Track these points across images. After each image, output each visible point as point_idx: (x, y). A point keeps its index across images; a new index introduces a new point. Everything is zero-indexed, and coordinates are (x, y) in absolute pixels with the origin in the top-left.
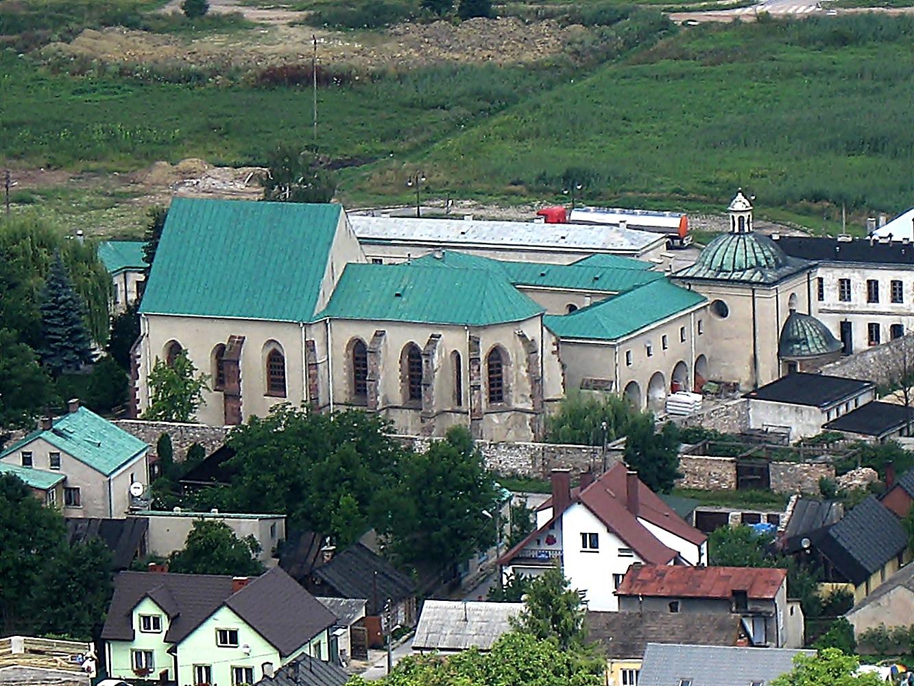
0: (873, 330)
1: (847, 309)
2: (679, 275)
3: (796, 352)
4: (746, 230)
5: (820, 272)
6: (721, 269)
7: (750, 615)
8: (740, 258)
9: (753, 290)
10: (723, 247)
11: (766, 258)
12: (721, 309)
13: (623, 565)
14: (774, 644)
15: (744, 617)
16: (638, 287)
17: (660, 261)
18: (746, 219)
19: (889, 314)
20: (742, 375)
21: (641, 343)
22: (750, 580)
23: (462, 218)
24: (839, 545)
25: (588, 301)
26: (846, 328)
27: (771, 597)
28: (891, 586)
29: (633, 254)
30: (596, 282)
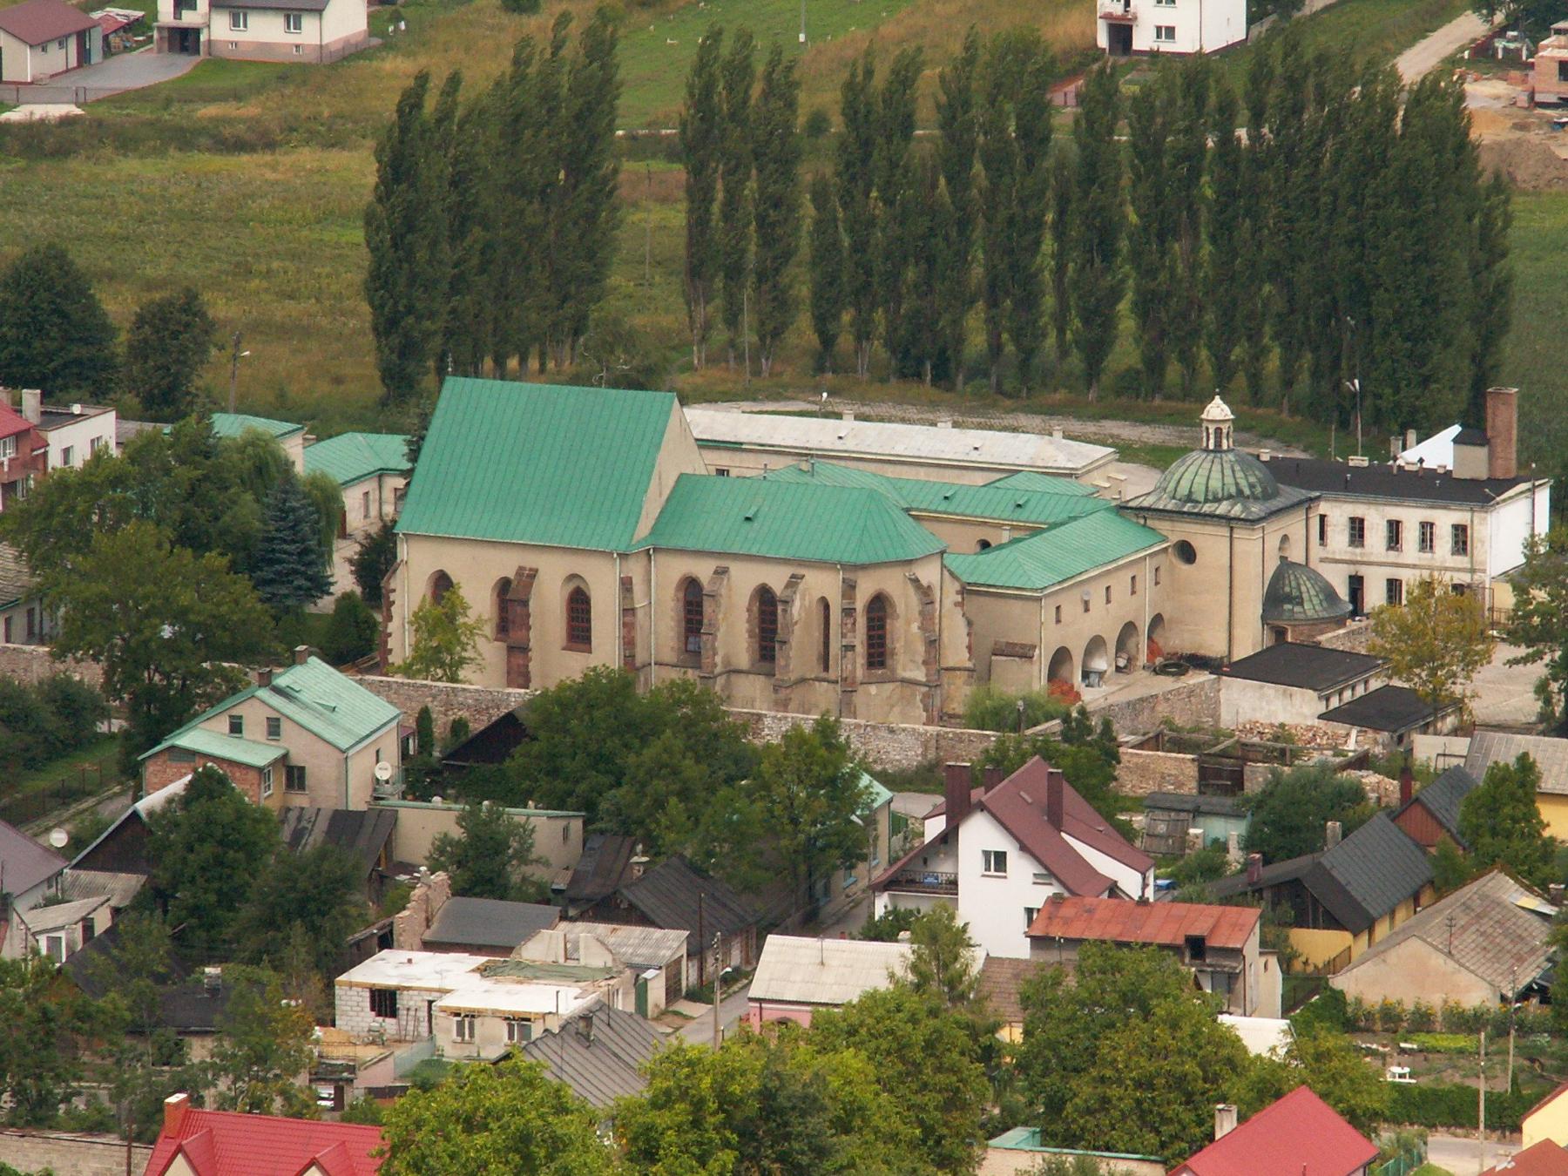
0: (1393, 586)
1: (1359, 559)
2: (1131, 504)
3: (1287, 615)
4: (1225, 447)
5: (1324, 507)
6: (1189, 498)
7: (1209, 969)
8: (1215, 484)
9: (1232, 529)
10: (1193, 469)
11: (1252, 486)
12: (1186, 552)
13: (1039, 896)
14: (1241, 1011)
15: (1201, 971)
16: (1075, 518)
17: (1107, 485)
18: (1225, 431)
19: (1414, 566)
20: (1215, 646)
21: (1076, 595)
22: (1210, 922)
23: (839, 416)
24: (1333, 878)
25: (1005, 536)
26: (1356, 583)
27: (1239, 946)
28: (1401, 937)
29: (1071, 474)
30: (1019, 510)
